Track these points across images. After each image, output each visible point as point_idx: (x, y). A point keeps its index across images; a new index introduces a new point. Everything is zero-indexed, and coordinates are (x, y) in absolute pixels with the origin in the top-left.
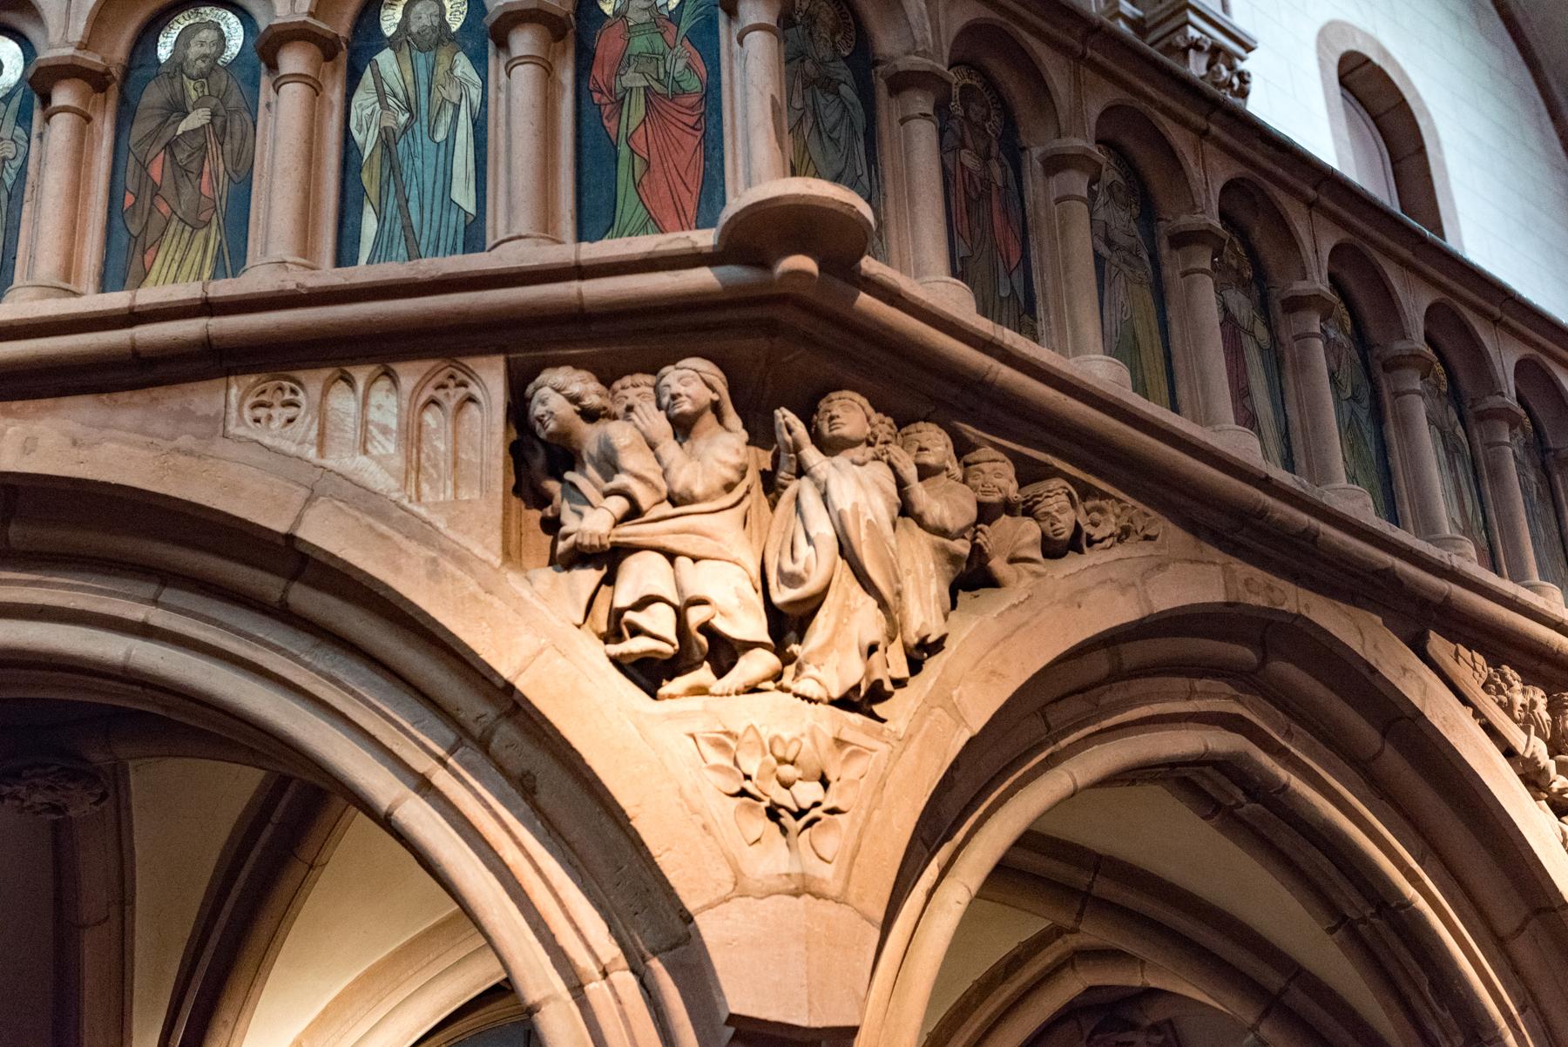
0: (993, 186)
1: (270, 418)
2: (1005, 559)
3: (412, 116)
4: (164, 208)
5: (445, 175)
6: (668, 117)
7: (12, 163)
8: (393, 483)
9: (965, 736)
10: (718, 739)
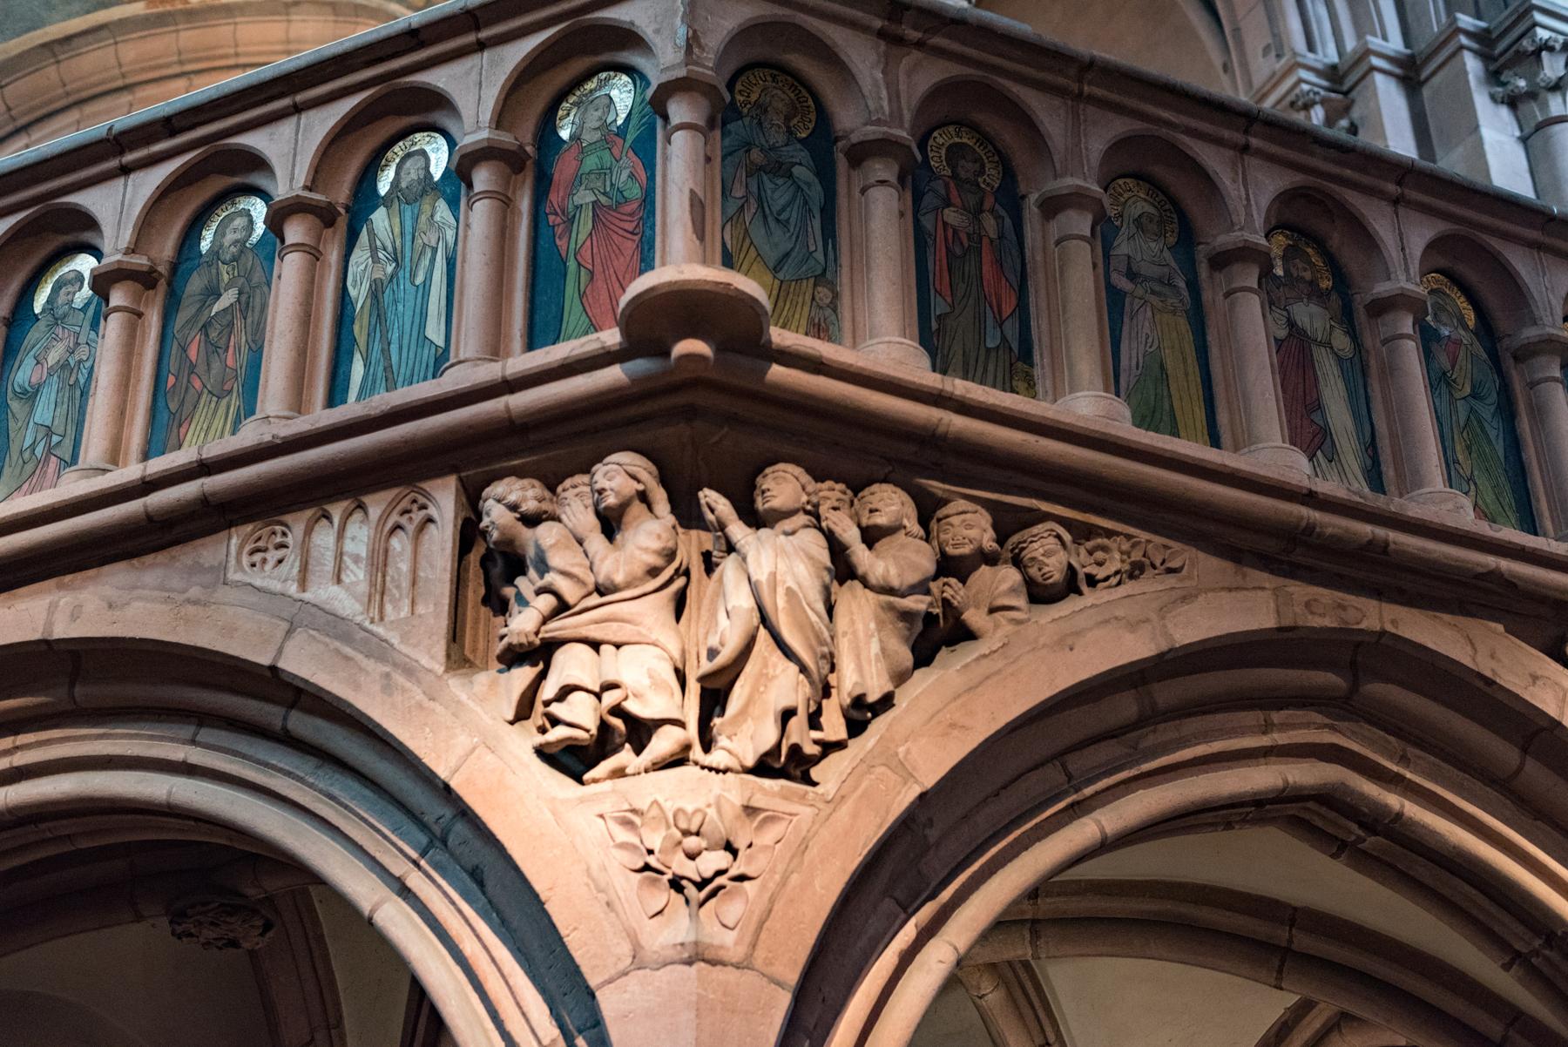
0: (985, 241)
1: (264, 561)
2: (986, 610)
3: (398, 264)
4: (197, 384)
5: (421, 313)
6: (612, 226)
8: (358, 607)
9: (915, 791)
10: (624, 817)
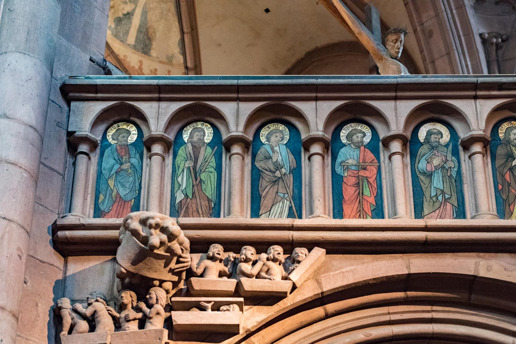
7: (454, 169)
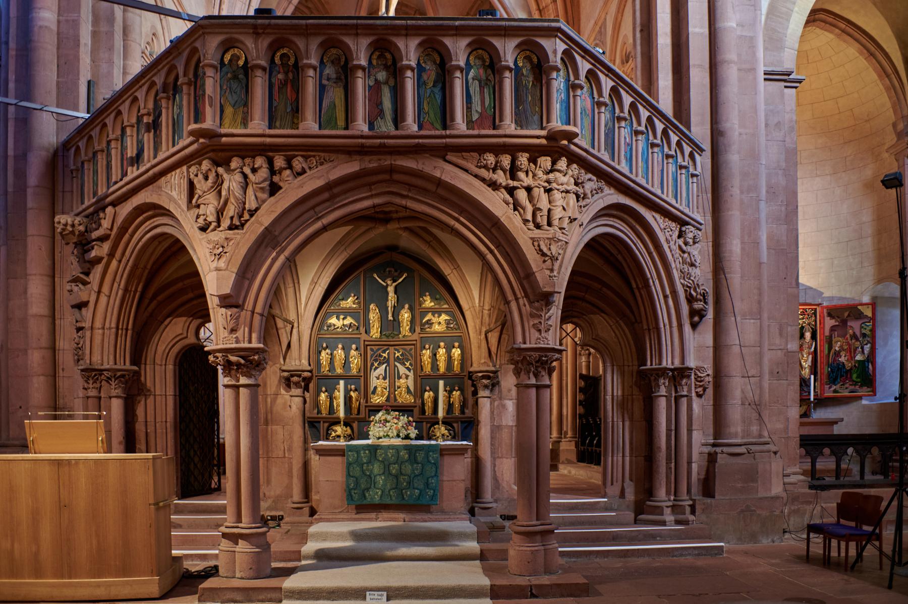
9: (264, 227)
